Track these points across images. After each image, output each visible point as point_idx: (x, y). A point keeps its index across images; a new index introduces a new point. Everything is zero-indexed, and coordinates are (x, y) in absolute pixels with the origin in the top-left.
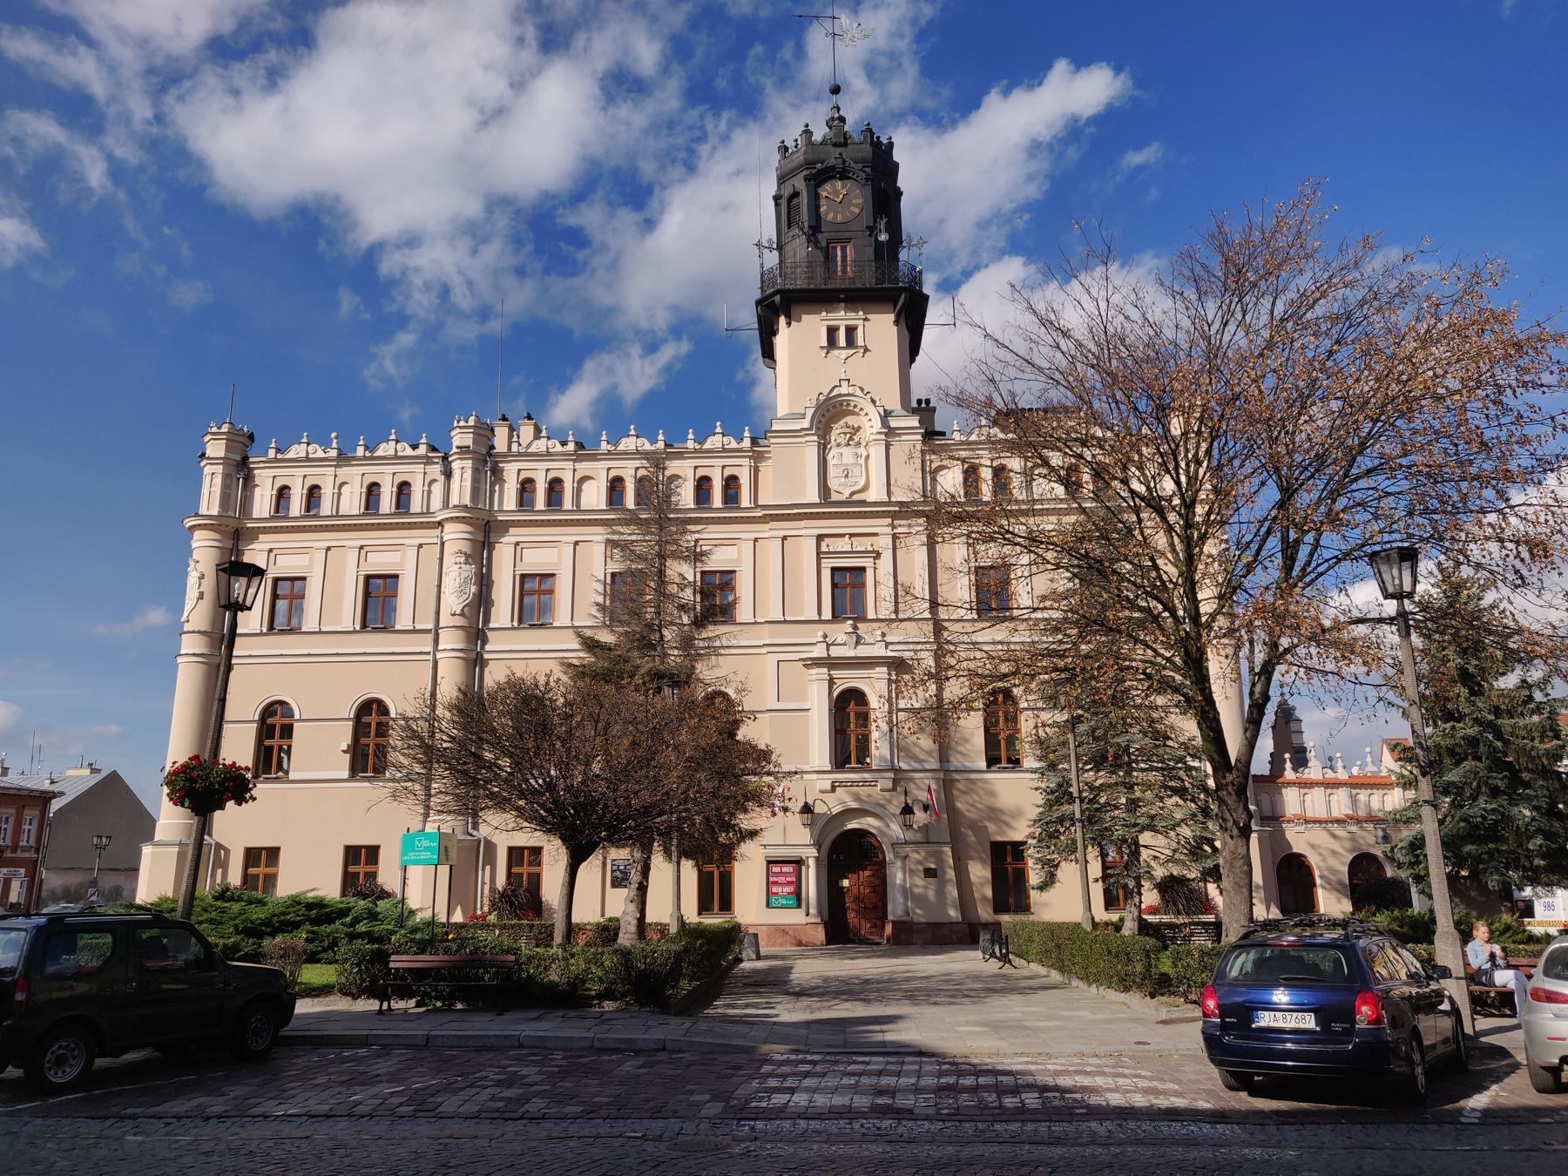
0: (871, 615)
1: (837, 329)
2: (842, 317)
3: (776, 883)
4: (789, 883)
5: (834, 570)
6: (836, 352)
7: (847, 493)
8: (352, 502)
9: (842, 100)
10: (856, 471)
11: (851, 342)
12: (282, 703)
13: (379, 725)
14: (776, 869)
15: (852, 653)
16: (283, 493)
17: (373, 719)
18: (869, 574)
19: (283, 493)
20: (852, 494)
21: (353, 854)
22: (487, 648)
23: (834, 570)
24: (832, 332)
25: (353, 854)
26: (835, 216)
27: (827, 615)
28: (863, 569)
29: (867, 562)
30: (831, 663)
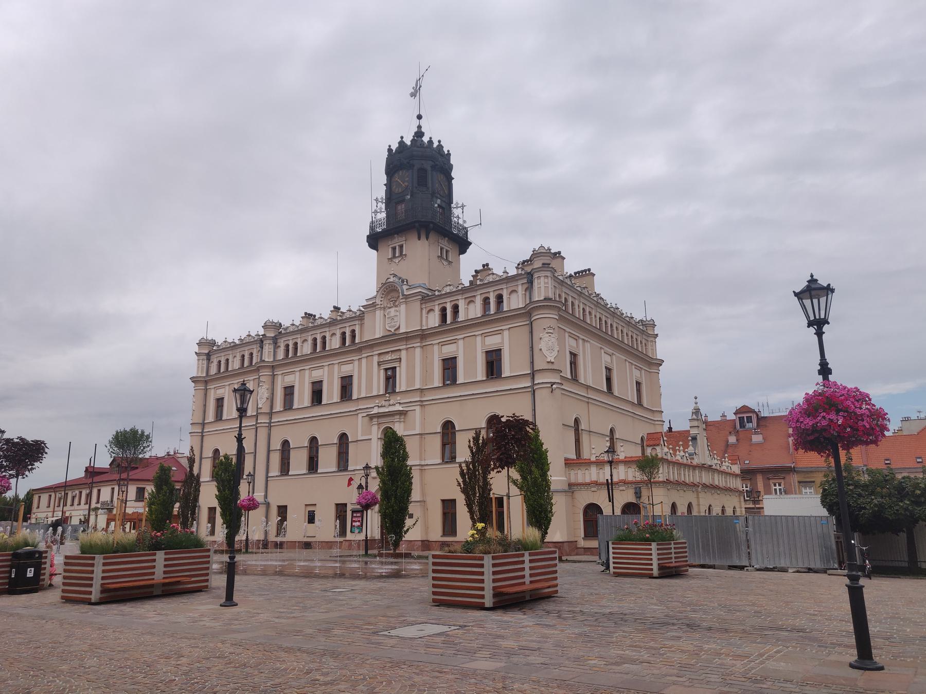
2: (397, 241)
23: (386, 370)
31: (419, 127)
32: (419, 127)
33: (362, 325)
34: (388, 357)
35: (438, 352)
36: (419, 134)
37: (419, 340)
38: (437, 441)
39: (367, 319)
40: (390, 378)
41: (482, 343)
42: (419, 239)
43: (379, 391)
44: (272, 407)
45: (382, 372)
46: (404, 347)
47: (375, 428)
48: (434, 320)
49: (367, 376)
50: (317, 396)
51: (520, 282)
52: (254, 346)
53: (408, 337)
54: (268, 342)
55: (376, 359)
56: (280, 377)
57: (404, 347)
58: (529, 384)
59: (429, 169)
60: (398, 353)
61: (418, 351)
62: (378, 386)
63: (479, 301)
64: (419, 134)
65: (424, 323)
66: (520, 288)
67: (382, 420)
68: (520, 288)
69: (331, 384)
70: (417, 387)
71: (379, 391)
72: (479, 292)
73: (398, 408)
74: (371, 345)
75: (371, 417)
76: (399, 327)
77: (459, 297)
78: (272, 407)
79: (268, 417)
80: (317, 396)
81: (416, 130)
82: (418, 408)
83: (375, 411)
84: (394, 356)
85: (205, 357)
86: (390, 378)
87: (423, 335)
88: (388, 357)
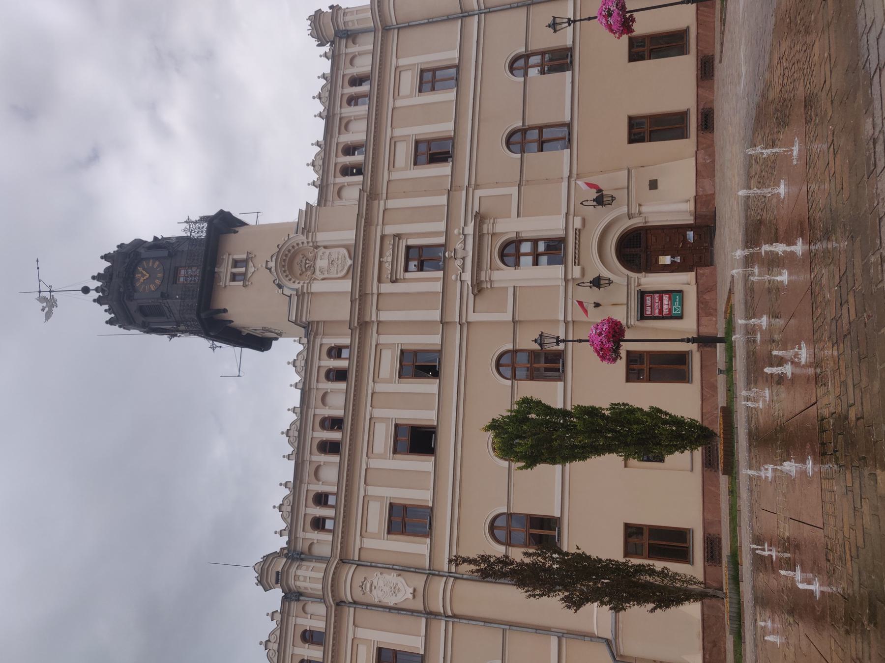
0: (441, 240)
2: (225, 270)
3: (661, 310)
4: (661, 299)
7: (350, 262)
10: (334, 256)
11: (245, 263)
14: (648, 311)
18: (412, 242)
20: (350, 258)
23: (406, 270)
24: (234, 277)
34: (387, 266)
35: (402, 168)
37: (377, 202)
38: (533, 158)
39: (319, 312)
40: (423, 258)
41: (406, 93)
43: (436, 279)
44: (417, 570)
45: (408, 275)
46: (379, 228)
47: (497, 275)
49: (411, 310)
50: (419, 440)
51: (343, 50)
53: (366, 221)
54: (293, 570)
55: (387, 288)
56: (368, 543)
57: (379, 228)
58: (476, 17)
61: (392, 204)
62: (428, 282)
63: (350, 111)
66: (349, 50)
68: (349, 50)
69: (407, 401)
70: (443, 200)
71: (436, 279)
72: (337, 110)
73: (470, 230)
74: (360, 297)
75: (478, 288)
76: (346, 247)
78: (417, 570)
79: (434, 623)
80: (419, 440)
82: (479, 193)
83: (467, 277)
84: (388, 244)
86: (423, 258)
87: (370, 195)
88: (387, 266)
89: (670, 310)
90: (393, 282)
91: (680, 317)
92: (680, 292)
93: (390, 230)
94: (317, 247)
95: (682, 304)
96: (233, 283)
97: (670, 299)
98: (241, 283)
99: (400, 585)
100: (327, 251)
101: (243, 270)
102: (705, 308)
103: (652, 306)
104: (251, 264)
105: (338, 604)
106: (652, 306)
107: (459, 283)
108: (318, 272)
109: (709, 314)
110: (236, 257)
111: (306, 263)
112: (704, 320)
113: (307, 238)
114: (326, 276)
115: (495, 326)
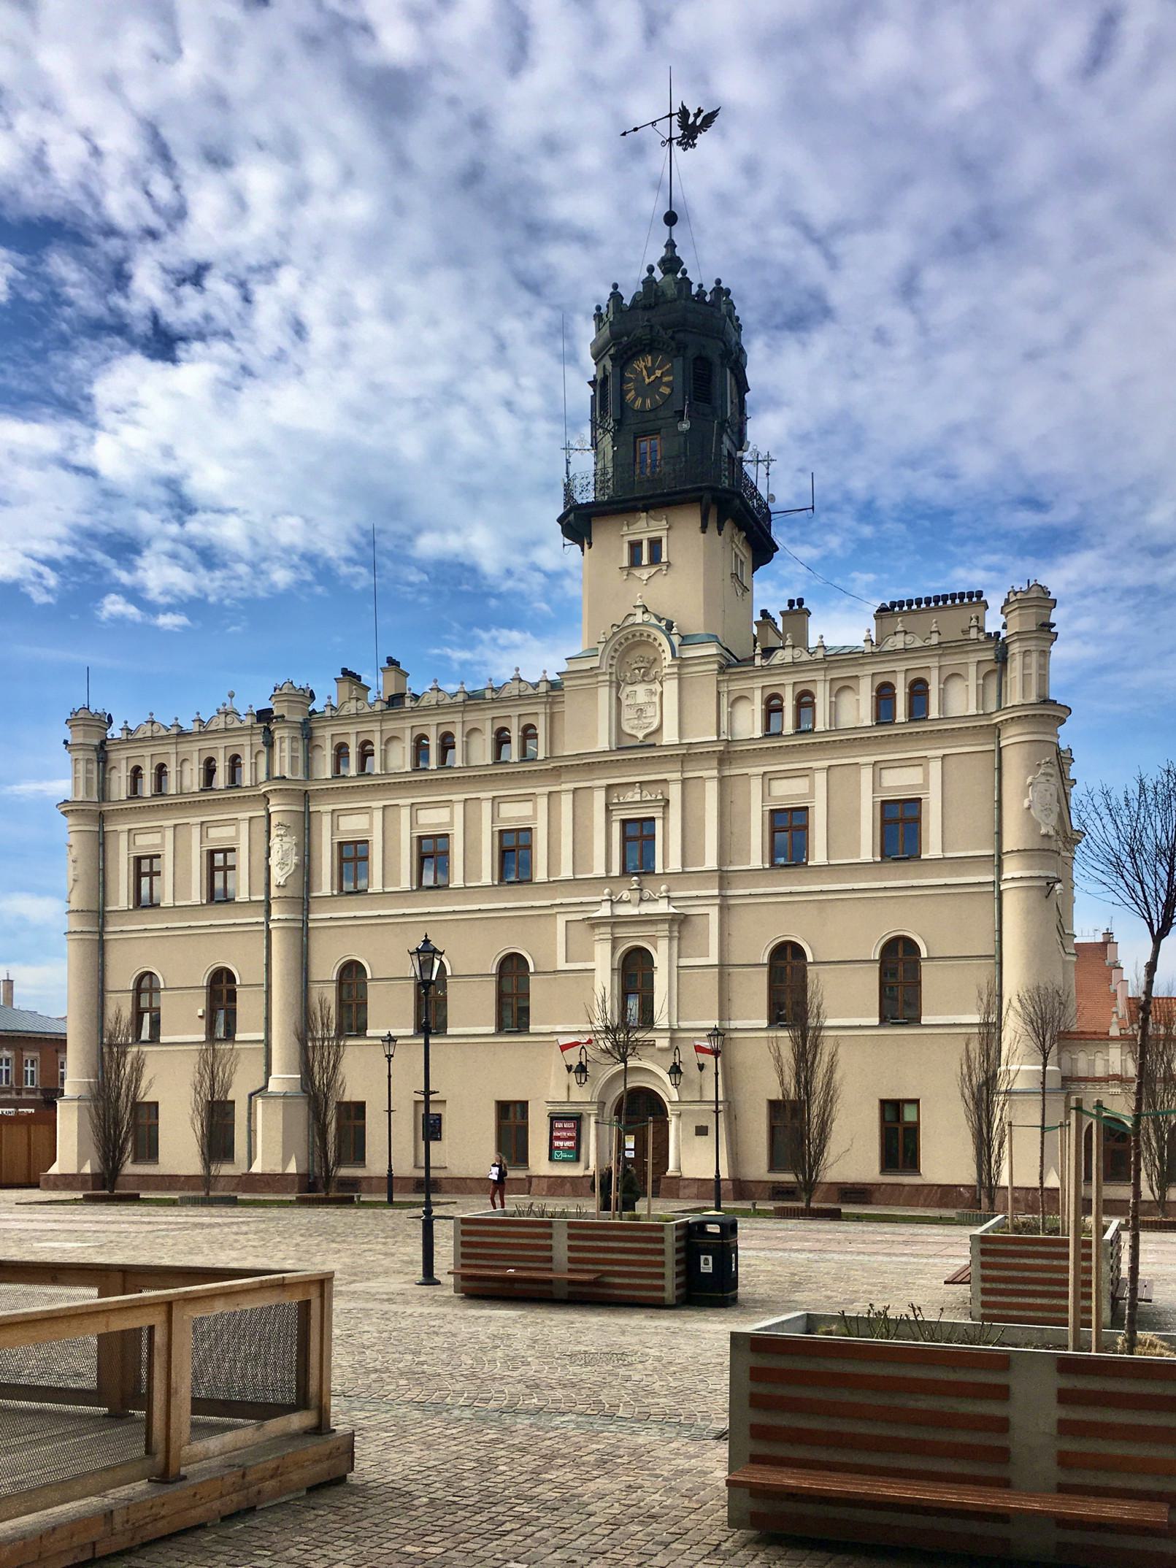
1: (640, 543)
2: (645, 528)
3: (558, 1138)
4: (570, 1139)
5: (624, 822)
6: (637, 572)
7: (640, 735)
8: (193, 779)
9: (678, 233)
10: (650, 711)
11: (655, 558)
12: (151, 974)
13: (228, 991)
14: (558, 1125)
15: (635, 911)
16: (136, 773)
17: (224, 987)
18: (659, 824)
19: (136, 773)
20: (646, 736)
21: (504, 1108)
22: (311, 916)
23: (624, 822)
24: (635, 547)
25: (504, 1108)
26: (644, 403)
27: (616, 871)
28: (653, 819)
29: (657, 813)
30: (615, 922)
31: (671, 245)
32: (671, 245)
33: (552, 718)
36: (671, 263)
42: (704, 529)
45: (616, 828)
48: (749, 722)
49: (575, 835)
52: (245, 741)
59: (717, 360)
60: (662, 786)
64: (671, 263)
65: (724, 726)
67: (620, 932)
74: (589, 765)
76: (659, 730)
77: (819, 676)
81: (662, 252)
85: (93, 756)
89: (558, 1148)
90: (607, 806)
91: (551, 1159)
92: (578, 1159)
93: (675, 792)
94: (661, 683)
95: (564, 1160)
96: (626, 546)
97: (570, 1148)
98: (626, 563)
99: (287, 868)
100: (656, 699)
101: (645, 561)
102: (557, 1186)
103: (563, 1129)
104: (653, 570)
105: (264, 795)
106: (563, 1129)
107: (598, 899)
108: (629, 689)
109: (549, 1188)
110: (664, 541)
111: (639, 669)
112: (545, 1183)
113: (670, 666)
114: (625, 702)
115: (550, 948)
